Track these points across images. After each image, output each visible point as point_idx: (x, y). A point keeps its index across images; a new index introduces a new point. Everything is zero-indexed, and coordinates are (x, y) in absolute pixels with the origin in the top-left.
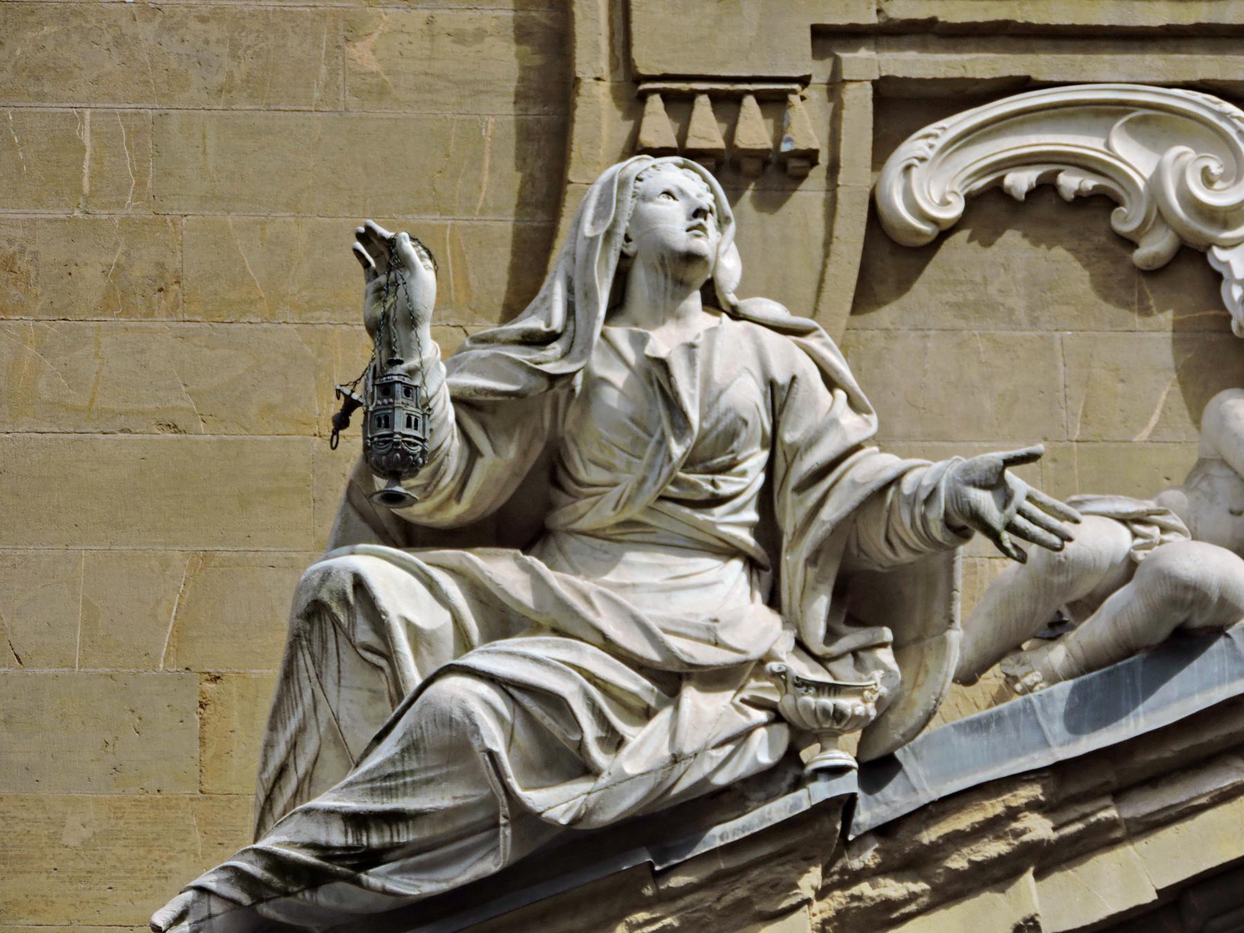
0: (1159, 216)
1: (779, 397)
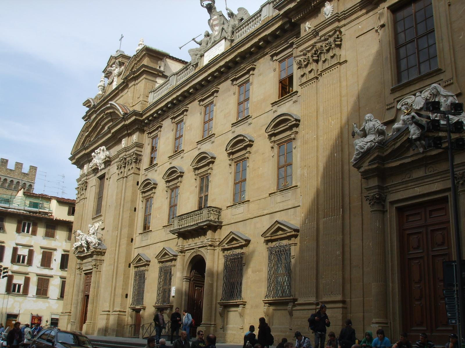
0: (410, 104)
1: (374, 125)
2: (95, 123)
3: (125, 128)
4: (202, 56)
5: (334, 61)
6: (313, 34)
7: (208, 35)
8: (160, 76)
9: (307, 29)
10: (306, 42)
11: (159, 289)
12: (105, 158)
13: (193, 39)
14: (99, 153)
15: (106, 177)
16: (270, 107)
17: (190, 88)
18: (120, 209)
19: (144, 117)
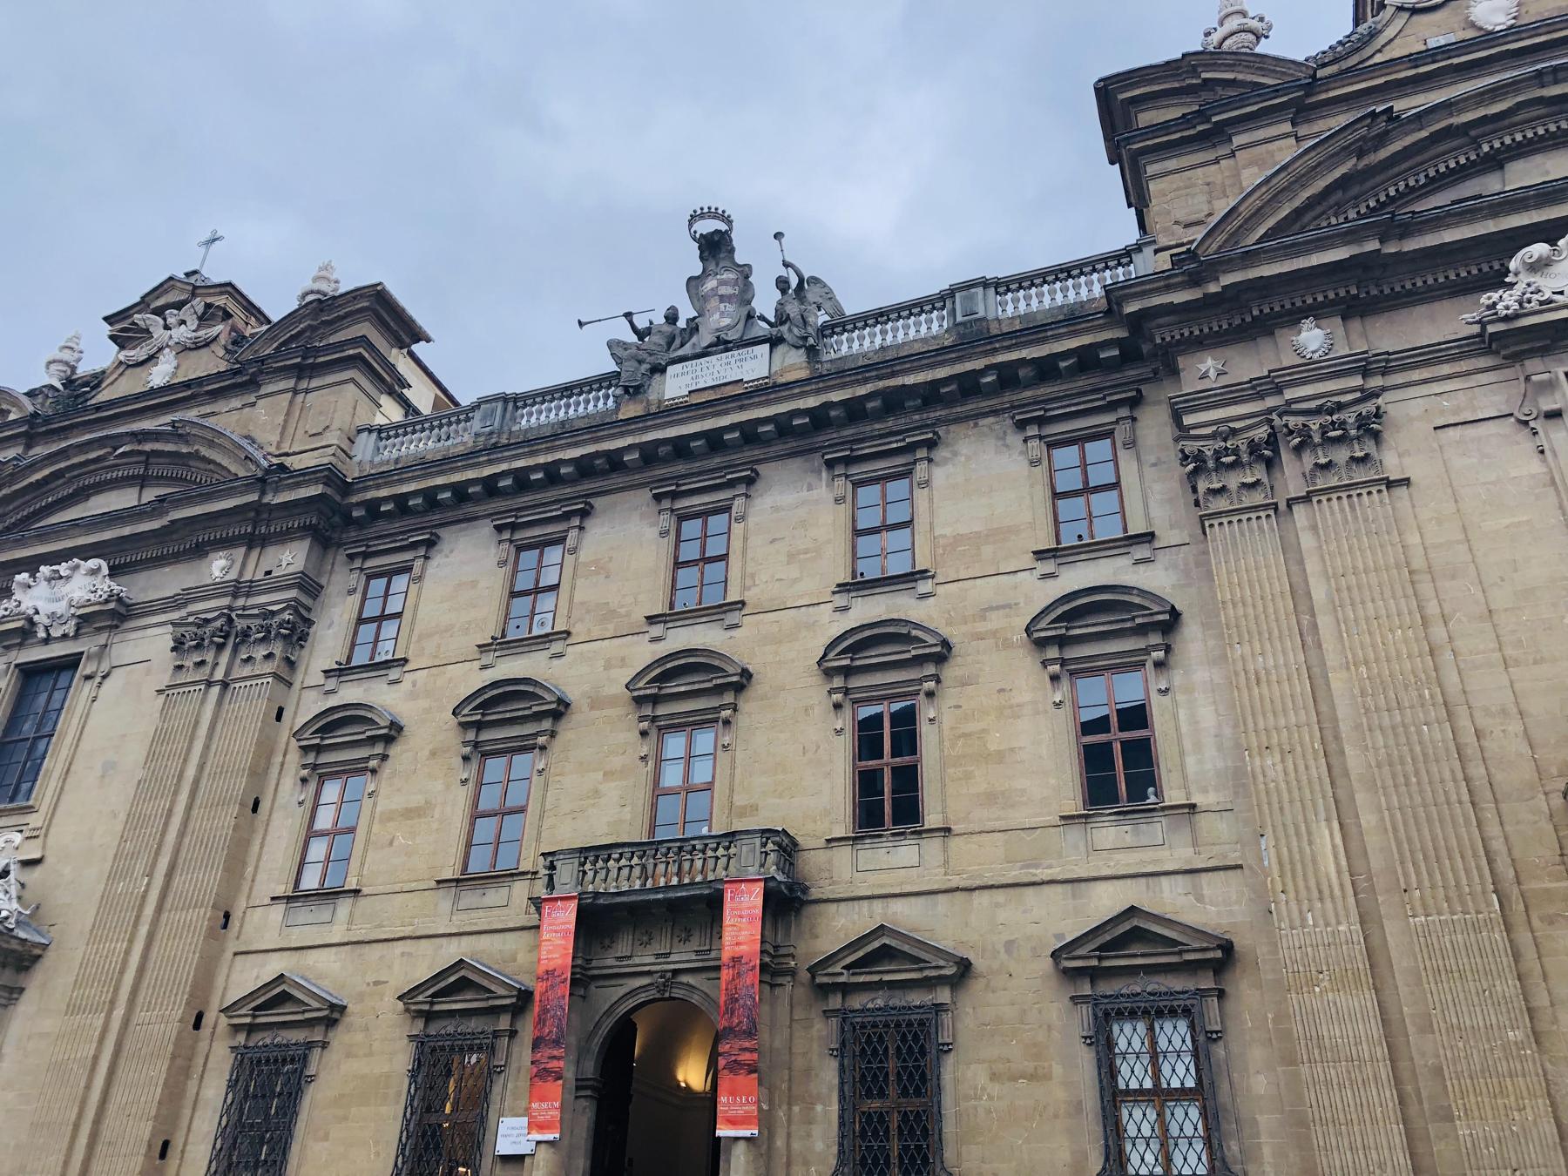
2: (46, 472)
3: (252, 514)
4: (659, 369)
5: (1360, 475)
6: (1253, 388)
7: (672, 317)
8: (391, 393)
9: (1212, 374)
10: (1215, 407)
11: (407, 1121)
12: (107, 601)
13: (628, 315)
14: (68, 578)
15: (86, 668)
16: (1028, 560)
17: (630, 448)
18: (176, 793)
19: (354, 499)
